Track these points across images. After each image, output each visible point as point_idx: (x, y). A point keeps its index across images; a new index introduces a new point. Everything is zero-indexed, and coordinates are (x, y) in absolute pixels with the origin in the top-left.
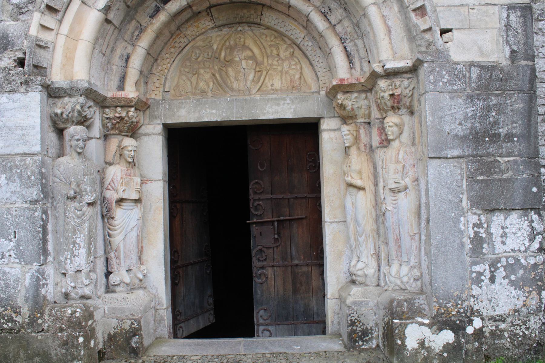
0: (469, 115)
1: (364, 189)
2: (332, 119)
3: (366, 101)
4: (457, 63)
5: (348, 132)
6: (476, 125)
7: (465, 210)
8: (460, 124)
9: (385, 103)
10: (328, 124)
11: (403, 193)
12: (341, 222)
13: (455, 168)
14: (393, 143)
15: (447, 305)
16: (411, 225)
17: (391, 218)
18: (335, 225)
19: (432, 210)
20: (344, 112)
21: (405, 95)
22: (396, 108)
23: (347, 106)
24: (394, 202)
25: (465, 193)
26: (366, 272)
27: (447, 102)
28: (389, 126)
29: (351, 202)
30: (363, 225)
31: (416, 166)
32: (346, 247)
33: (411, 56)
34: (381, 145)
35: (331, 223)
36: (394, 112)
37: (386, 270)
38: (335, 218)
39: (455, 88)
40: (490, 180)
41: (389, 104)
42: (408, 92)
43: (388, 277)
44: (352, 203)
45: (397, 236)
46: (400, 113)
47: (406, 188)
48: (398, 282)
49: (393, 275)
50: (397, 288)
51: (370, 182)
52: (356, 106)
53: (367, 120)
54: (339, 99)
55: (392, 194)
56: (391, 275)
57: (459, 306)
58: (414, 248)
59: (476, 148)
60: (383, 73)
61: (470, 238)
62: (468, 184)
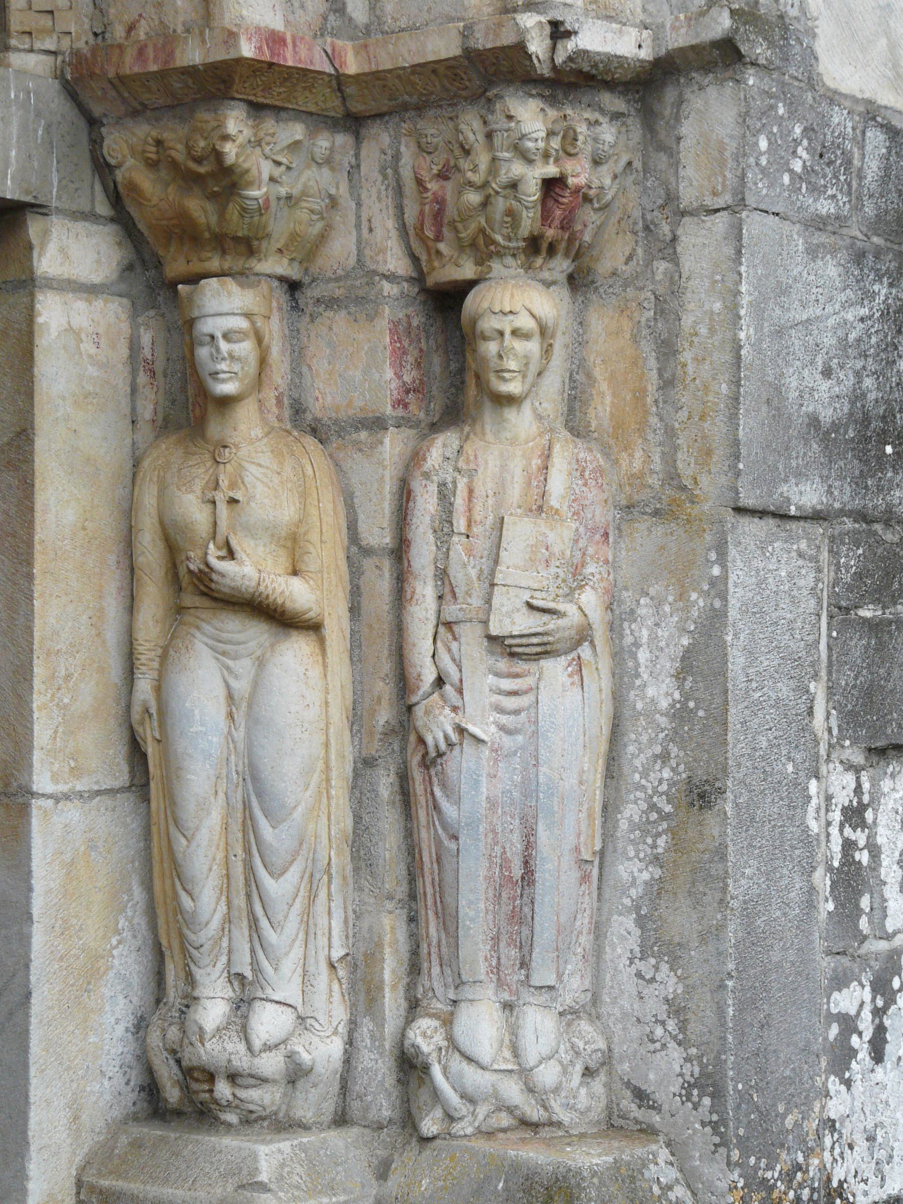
0: (852, 337)
1: (314, 627)
2: (81, 227)
3: (326, 171)
4: (833, 97)
5: (242, 323)
6: (868, 382)
7: (823, 750)
8: (827, 373)
9: (510, 213)
10: (63, 251)
11: (563, 661)
12: (99, 793)
13: (801, 562)
14: (510, 414)
15: (769, 1175)
16: (590, 816)
17: (484, 780)
18: (72, 813)
19: (735, 746)
20: (210, 207)
21: (592, 193)
22: (545, 246)
23: (249, 184)
24: (511, 703)
25: (823, 674)
26: (305, 1057)
27: (800, 268)
28: (515, 333)
29: (221, 692)
30: (298, 814)
31: (611, 539)
32: (118, 932)
33: (644, 10)
34: (400, 412)
35: (57, 798)
36: (528, 267)
37: (424, 1035)
38: (76, 772)
39: (825, 207)
40: (890, 622)
41: (529, 221)
42: (607, 181)
43: (445, 1071)
44: (230, 697)
45: (505, 864)
46: (546, 275)
47: (584, 635)
48: (513, 1091)
49: (486, 1059)
50: (505, 1120)
51: (341, 594)
52: (283, 191)
53: (294, 273)
54: (226, 138)
55: (503, 664)
56: (470, 1059)
57: (799, 1175)
58: (584, 921)
59: (859, 483)
60: (544, 70)
61: (830, 869)
62: (834, 634)
